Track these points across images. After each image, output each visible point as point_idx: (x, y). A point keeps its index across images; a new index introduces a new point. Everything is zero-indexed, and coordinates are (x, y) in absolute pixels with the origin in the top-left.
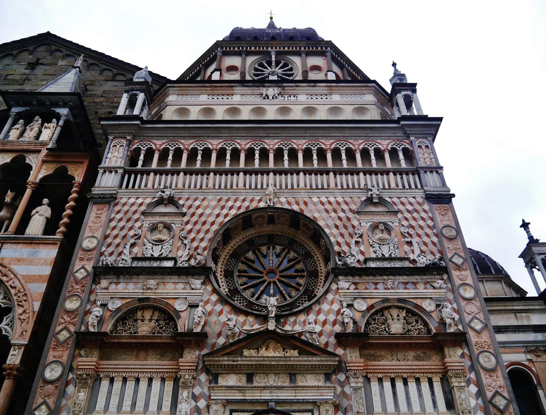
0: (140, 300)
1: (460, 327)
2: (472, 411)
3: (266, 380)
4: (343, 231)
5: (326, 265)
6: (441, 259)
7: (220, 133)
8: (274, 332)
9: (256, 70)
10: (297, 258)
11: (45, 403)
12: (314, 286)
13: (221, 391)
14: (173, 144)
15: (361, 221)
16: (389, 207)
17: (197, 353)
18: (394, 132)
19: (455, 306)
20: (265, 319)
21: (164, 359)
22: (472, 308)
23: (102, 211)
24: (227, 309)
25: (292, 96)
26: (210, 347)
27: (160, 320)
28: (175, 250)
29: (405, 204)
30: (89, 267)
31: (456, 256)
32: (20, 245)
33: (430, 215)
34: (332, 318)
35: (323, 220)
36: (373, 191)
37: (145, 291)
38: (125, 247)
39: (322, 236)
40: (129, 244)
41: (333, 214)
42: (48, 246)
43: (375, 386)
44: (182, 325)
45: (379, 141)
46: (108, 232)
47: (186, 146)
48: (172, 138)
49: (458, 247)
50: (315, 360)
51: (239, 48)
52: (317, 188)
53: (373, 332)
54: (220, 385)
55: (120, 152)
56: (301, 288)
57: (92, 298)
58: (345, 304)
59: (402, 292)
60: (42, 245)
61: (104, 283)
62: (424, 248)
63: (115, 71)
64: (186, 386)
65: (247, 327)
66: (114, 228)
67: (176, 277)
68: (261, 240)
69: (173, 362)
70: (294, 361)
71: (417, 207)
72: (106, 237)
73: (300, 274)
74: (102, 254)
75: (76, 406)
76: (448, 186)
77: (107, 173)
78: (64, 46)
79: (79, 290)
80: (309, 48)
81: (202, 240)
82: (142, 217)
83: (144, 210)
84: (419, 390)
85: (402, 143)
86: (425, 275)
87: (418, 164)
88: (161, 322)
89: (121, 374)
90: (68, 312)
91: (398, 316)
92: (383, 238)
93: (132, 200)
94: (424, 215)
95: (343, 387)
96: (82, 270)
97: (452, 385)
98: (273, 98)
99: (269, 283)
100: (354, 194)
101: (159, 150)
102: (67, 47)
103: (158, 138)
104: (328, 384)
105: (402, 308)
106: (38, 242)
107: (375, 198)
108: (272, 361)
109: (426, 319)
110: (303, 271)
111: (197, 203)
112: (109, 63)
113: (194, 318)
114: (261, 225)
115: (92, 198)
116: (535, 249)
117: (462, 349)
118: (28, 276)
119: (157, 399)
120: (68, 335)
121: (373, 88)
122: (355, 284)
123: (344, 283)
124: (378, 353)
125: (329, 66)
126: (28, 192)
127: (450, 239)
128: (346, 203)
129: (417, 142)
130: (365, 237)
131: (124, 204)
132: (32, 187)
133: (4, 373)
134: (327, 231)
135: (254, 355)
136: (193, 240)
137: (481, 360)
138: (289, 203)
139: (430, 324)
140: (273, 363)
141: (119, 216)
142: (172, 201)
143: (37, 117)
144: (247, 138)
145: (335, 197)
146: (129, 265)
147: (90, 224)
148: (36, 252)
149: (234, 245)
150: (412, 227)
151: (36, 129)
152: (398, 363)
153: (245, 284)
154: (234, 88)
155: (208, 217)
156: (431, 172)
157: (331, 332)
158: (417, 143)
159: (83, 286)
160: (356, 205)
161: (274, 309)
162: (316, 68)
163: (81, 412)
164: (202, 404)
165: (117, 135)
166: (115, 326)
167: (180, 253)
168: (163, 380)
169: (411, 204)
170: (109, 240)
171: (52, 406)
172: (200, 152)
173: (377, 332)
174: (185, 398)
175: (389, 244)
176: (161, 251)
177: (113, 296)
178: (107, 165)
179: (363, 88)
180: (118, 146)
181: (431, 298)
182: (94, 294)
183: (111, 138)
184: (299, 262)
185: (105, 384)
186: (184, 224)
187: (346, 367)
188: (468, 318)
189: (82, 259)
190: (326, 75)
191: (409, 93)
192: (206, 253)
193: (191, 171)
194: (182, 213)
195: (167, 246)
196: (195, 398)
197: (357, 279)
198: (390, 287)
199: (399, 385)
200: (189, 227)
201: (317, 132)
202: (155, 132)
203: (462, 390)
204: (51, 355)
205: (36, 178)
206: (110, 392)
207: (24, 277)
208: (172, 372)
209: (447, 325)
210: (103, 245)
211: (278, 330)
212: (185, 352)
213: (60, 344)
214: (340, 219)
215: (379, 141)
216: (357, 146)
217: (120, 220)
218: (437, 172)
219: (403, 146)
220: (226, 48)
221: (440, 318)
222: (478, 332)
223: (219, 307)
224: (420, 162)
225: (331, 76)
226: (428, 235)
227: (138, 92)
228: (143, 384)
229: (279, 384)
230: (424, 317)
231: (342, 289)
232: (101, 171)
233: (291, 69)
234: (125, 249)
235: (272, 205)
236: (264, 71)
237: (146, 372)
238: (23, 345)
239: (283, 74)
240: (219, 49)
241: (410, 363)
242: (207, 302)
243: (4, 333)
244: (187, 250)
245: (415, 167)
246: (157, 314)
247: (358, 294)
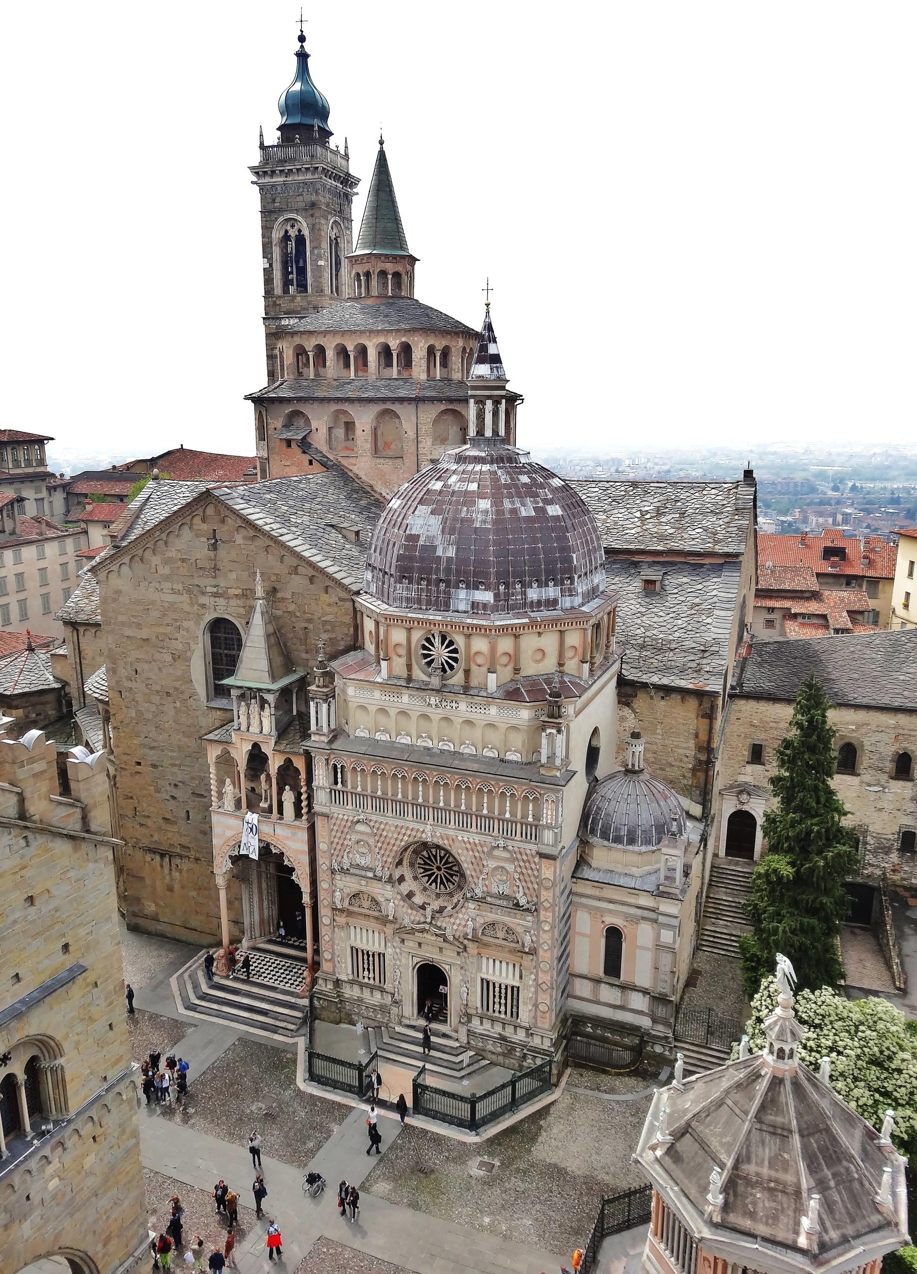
4: (476, 867)
34: (463, 923)
41: (471, 853)
43: (484, 960)
45: (516, 787)
59: (506, 919)
62: (527, 891)
66: (335, 837)
71: (531, 858)
72: (332, 843)
90: (324, 890)
93: (341, 816)
94: (533, 866)
111: (382, 826)
123: (471, 905)
127: (547, 889)
131: (337, 819)
134: (465, 865)
136: (383, 855)
141: (336, 828)
151: (257, 716)
164: (398, 951)
169: (526, 855)
170: (334, 845)
183: (313, 755)
185: (352, 928)
188: (541, 941)
195: (368, 858)
199: (497, 963)
200: (379, 845)
213: (325, 907)
222: (546, 951)
223: (402, 903)
226: (532, 883)
228: (370, 932)
236: (430, 650)
242: (396, 898)
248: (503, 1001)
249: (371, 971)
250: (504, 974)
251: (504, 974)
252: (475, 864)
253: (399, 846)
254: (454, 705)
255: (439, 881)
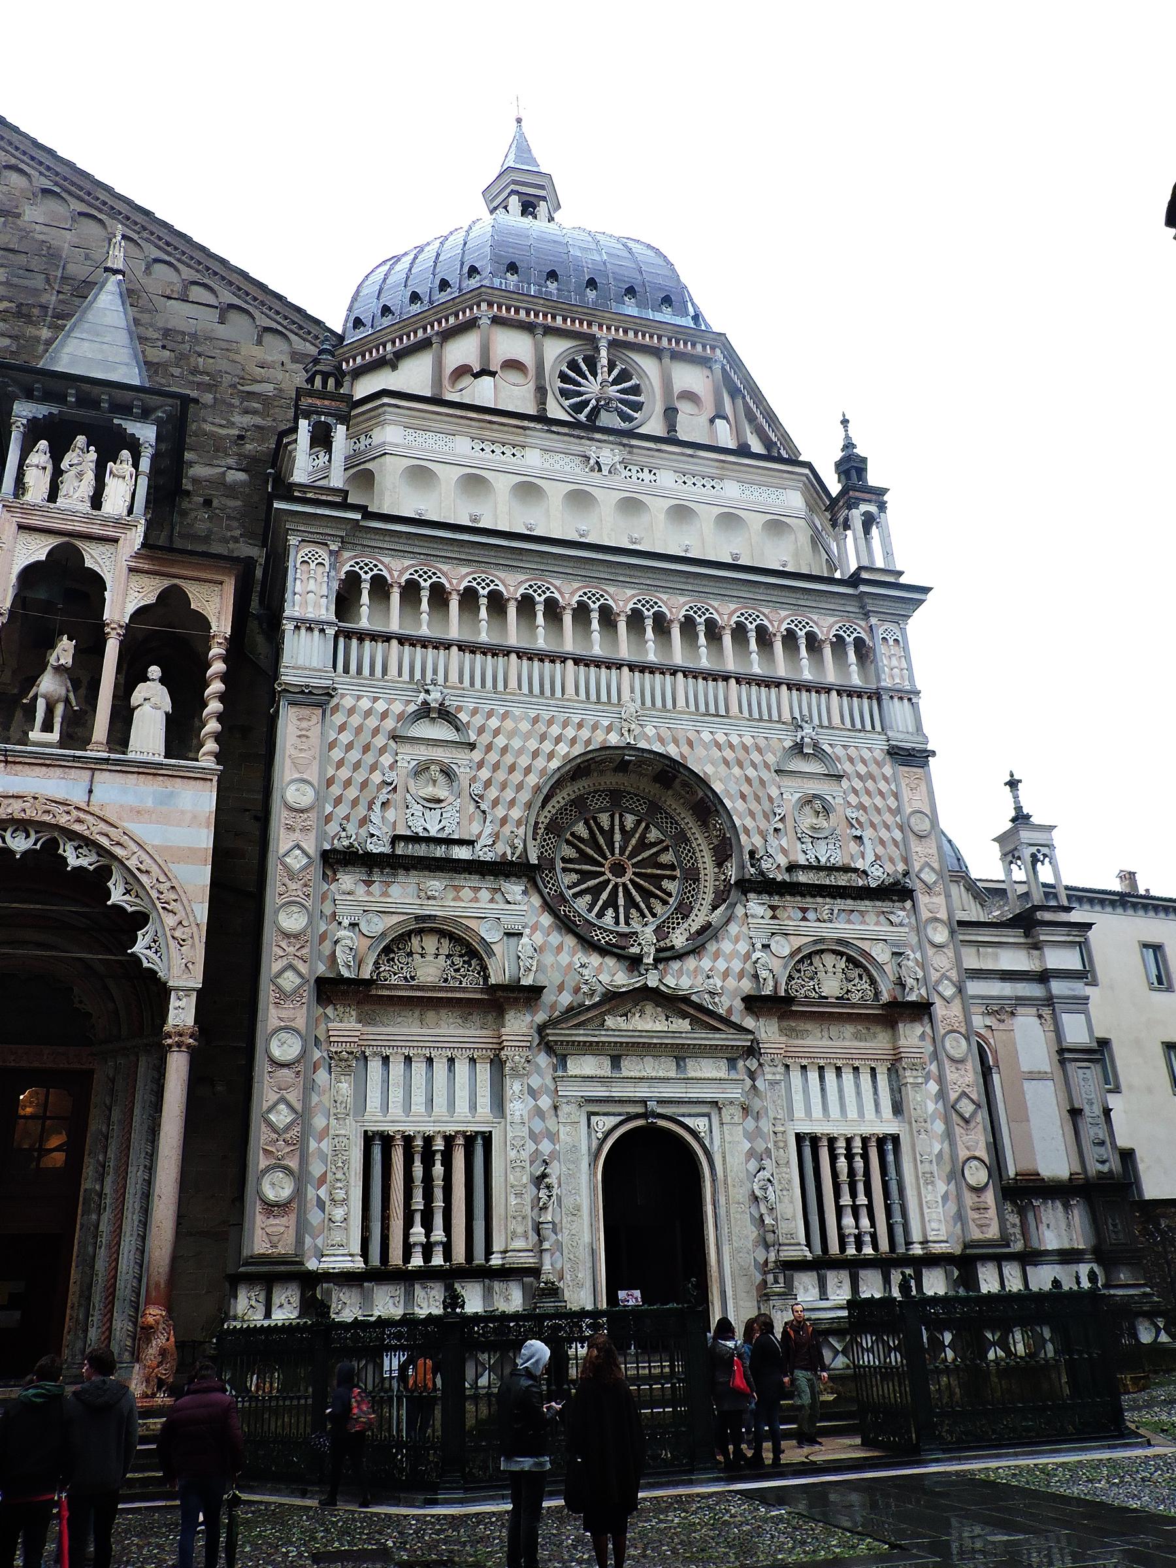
0: (419, 918)
1: (923, 992)
2: (928, 1120)
3: (641, 1066)
4: (754, 806)
5: (720, 864)
6: (906, 874)
7: (522, 560)
8: (656, 990)
9: (564, 377)
10: (662, 841)
11: (283, 1100)
12: (693, 896)
13: (575, 1084)
14: (425, 573)
15: (783, 790)
16: (827, 763)
17: (528, 1018)
18: (843, 602)
19: (918, 955)
20: (634, 963)
21: (468, 1026)
22: (942, 962)
23: (311, 723)
24: (570, 941)
25: (646, 470)
26: (548, 1009)
27: (451, 955)
28: (465, 822)
29: (855, 762)
30: (310, 846)
31: (927, 869)
32: (130, 776)
33: (893, 787)
34: (737, 965)
35: (720, 780)
36: (805, 731)
37: (425, 902)
38: (370, 808)
39: (717, 810)
40: (378, 804)
41: (736, 770)
42: (192, 782)
43: (796, 1076)
44: (499, 972)
45: (815, 617)
46: (331, 772)
47: (455, 581)
48: (422, 557)
49: (930, 851)
50: (716, 1039)
51: (528, 314)
52: (707, 714)
53: (797, 991)
54: (570, 1073)
55: (319, 580)
56: (671, 900)
57: (328, 909)
58: (759, 946)
60: (179, 780)
61: (347, 880)
62: (880, 850)
63: (187, 273)
64: (516, 1074)
65: (605, 978)
66: (340, 764)
67: (477, 877)
68: (598, 800)
69: (484, 1032)
70: (686, 1038)
71: (873, 768)
72: (330, 782)
73: (668, 873)
74: (328, 819)
75: (338, 1105)
76: (925, 731)
77: (303, 631)
78: (33, 158)
79: (300, 893)
80: (677, 343)
81: (512, 803)
82: (391, 742)
83: (395, 729)
84: (857, 1086)
85: (855, 626)
86: (878, 900)
87: (879, 680)
88: (457, 960)
89: (399, 1050)
90: (287, 935)
91: (834, 967)
92: (817, 827)
93: (365, 704)
94: (883, 785)
95: (753, 1080)
96: (298, 852)
97: (904, 1081)
98: (610, 472)
99: (616, 886)
100: (772, 732)
101: (400, 586)
102: (41, 163)
103: (393, 553)
104: (733, 1075)
105: (841, 954)
106: (170, 773)
107: (808, 745)
108: (652, 1037)
109: (875, 974)
110: (672, 867)
111: (494, 723)
112: (168, 244)
113: (519, 957)
114: (602, 772)
115: (285, 690)
116: (1025, 835)
117: (922, 1025)
118: (167, 848)
119: (466, 1094)
120: (298, 981)
121: (805, 479)
122: (773, 908)
123: (756, 906)
124: (802, 1026)
125: (719, 403)
126: (112, 649)
128: (759, 750)
129: (881, 631)
130: (789, 821)
131: (351, 711)
132: (118, 634)
133: (169, 1041)
134: (726, 801)
135: (624, 1026)
136: (495, 803)
137: (948, 1045)
138: (661, 740)
139: (881, 983)
140: (655, 1041)
141: (345, 738)
142: (445, 714)
143: (81, 440)
144: (573, 577)
145: (740, 735)
146: (387, 850)
147: (289, 750)
148: (171, 795)
149: (553, 807)
150: (862, 807)
151: (90, 476)
152: (830, 1043)
153: (575, 885)
154: (528, 432)
155: (517, 757)
156: (901, 698)
157: (737, 989)
158: (880, 632)
159: (306, 886)
160: (774, 754)
161: (653, 950)
162: (689, 396)
163: (348, 1115)
164: (545, 1102)
165: (310, 537)
166: (377, 964)
167: (475, 829)
168: (473, 1060)
169: (864, 762)
170: (336, 790)
171: (298, 1106)
172: (483, 601)
173: (803, 992)
174: (517, 1092)
175: (826, 838)
176: (440, 821)
177: (366, 908)
178: (297, 614)
179: (785, 475)
180: (313, 566)
181: (885, 940)
182: (328, 902)
183: (293, 540)
184: (666, 849)
185: (375, 1065)
186: (475, 767)
187: (760, 1049)
188: (935, 976)
189: (290, 828)
190: (712, 421)
191: (873, 509)
192: (521, 831)
193: (473, 646)
194: (470, 744)
196: (533, 1093)
197: (776, 900)
198: (826, 917)
199: (830, 1076)
200: (484, 774)
201: (706, 583)
202: (387, 539)
203: (917, 1089)
204: (271, 1015)
205: (123, 612)
206: (386, 1081)
207: (161, 849)
208: (486, 1049)
209: (907, 990)
210: (325, 800)
211: (663, 988)
212: (507, 1017)
213: (284, 996)
214: (748, 780)
215: (815, 617)
216: (776, 624)
217: (349, 747)
218: (910, 699)
219: (855, 635)
220: (500, 308)
221: (897, 976)
223: (555, 938)
224: (883, 676)
225: (725, 436)
227: (331, 420)
228: (440, 1067)
229: (661, 1074)
230: (873, 972)
231: (753, 916)
232: (288, 626)
233: (636, 390)
234: (372, 814)
235: (633, 743)
236: (579, 385)
237: (442, 1048)
238: (193, 989)
239: (622, 401)
240: (484, 306)
241: (847, 1044)
242: (535, 928)
243: (146, 964)
244: (487, 823)
245: (874, 687)
246: (446, 944)
247: (778, 927)
248: (862, 1200)
249: (438, 1220)
250: (852, 1113)
251: (852, 1113)
252: (750, 798)
253: (543, 772)
254: (646, 475)
255: (621, 901)
